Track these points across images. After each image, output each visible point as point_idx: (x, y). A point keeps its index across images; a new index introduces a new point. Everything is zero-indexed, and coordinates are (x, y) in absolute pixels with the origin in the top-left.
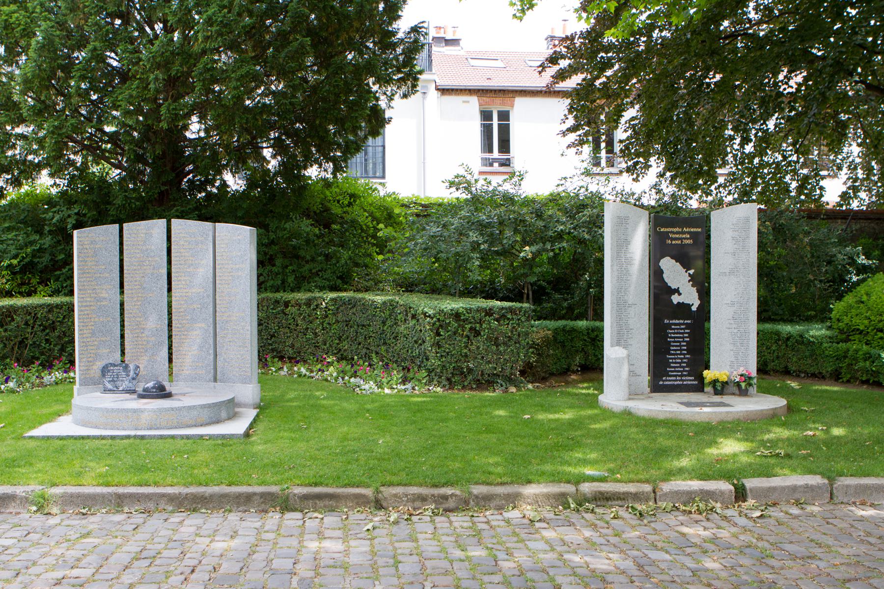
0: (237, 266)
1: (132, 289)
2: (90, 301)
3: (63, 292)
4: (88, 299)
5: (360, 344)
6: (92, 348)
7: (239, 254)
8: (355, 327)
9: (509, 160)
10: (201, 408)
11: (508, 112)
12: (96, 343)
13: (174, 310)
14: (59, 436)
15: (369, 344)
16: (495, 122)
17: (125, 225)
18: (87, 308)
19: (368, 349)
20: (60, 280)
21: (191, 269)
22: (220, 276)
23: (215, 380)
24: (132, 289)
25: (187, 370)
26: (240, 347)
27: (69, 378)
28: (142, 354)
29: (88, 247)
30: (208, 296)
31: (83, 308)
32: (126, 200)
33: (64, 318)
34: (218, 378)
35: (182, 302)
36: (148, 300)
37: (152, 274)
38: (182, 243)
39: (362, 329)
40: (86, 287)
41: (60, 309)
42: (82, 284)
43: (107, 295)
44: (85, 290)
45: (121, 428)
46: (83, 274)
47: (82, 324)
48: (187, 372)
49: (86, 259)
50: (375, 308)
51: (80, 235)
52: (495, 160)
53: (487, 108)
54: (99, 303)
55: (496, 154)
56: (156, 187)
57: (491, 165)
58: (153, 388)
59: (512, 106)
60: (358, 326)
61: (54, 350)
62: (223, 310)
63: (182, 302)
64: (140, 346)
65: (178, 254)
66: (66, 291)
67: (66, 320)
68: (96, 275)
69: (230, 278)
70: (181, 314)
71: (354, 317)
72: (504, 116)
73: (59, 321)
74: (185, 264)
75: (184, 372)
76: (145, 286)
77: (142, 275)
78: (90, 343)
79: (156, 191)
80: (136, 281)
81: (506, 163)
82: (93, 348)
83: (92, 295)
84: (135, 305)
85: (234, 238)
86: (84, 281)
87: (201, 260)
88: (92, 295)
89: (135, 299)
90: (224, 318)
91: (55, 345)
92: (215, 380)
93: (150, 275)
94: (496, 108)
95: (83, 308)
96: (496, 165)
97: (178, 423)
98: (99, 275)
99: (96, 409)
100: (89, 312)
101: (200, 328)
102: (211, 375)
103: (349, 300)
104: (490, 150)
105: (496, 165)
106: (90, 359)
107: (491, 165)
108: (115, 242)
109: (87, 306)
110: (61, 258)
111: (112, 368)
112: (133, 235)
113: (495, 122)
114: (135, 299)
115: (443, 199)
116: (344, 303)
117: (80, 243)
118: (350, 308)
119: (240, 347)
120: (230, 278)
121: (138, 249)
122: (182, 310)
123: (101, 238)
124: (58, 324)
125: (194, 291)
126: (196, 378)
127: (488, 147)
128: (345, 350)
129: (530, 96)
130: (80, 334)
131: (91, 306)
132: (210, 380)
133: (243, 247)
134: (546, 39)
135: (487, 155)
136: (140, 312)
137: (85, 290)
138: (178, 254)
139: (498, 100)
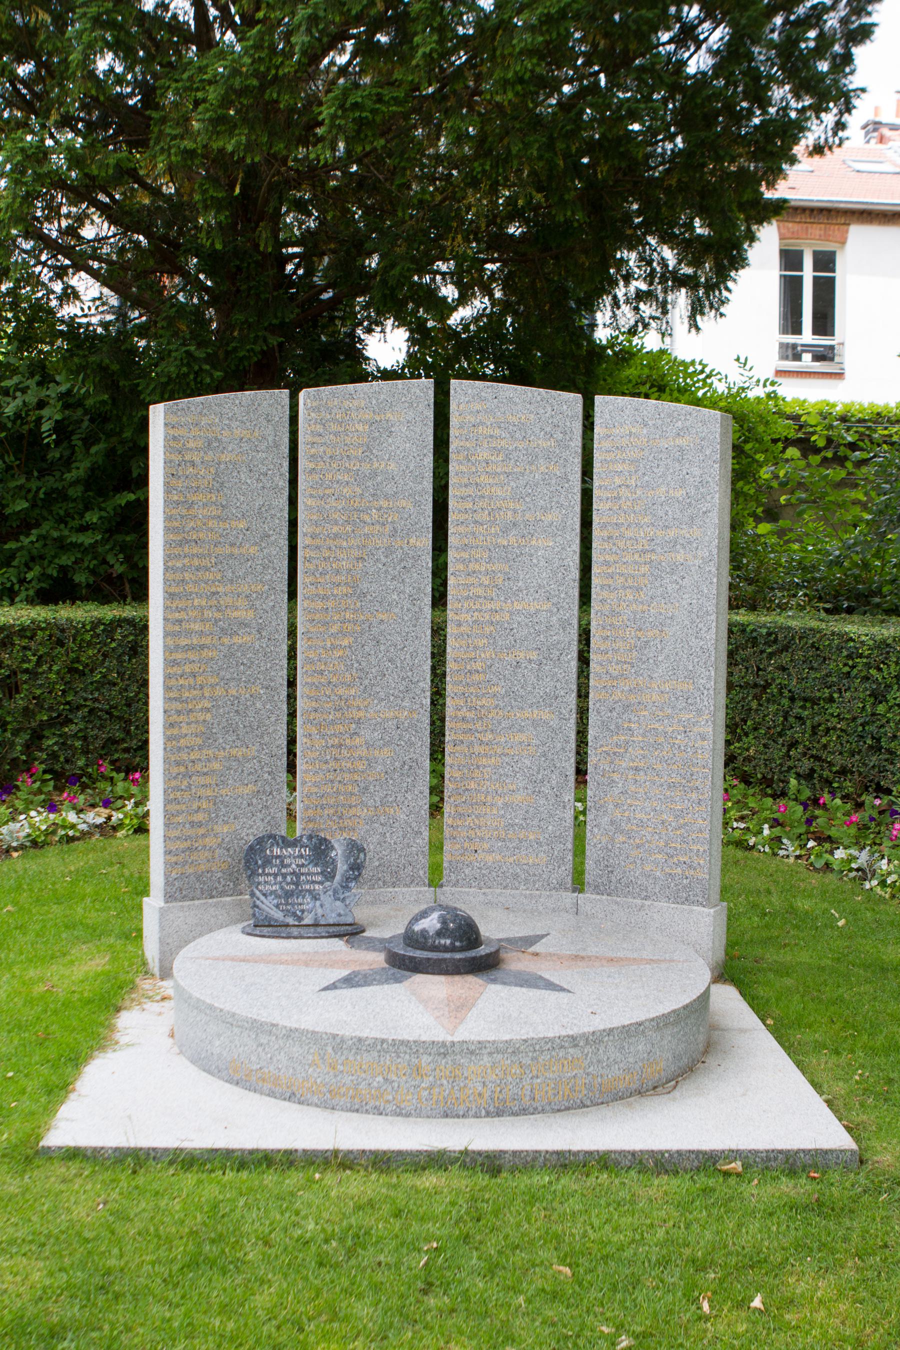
0: (672, 533)
1: (325, 598)
2: (201, 633)
3: (23, 595)
4: (197, 627)
5: (793, 744)
6: (203, 780)
7: (679, 494)
8: (785, 702)
9: (832, 348)
10: (658, 1028)
11: (833, 254)
12: (216, 766)
13: (451, 666)
14: (178, 1151)
15: (825, 747)
16: (808, 274)
17: (302, 395)
18: (191, 655)
19: (817, 758)
20: (15, 563)
21: (512, 539)
22: (607, 563)
23: (578, 884)
24: (325, 598)
25: (490, 851)
26: (671, 786)
27: (64, 827)
28: (353, 801)
29: (197, 460)
30: (564, 625)
31: (179, 656)
32: (188, 365)
33: (39, 663)
34: (588, 878)
35: (481, 642)
36: (374, 631)
37: (389, 551)
38: (484, 454)
39: (803, 707)
40: (190, 588)
41: (31, 638)
42: (179, 576)
43: (251, 614)
44: (188, 596)
45: (390, 1107)
46: (180, 544)
47: (178, 705)
48: (490, 858)
49: (192, 498)
50: (849, 657)
51: (174, 419)
52: (807, 348)
53: (793, 245)
54: (226, 640)
55: (807, 336)
56: (257, 337)
57: (797, 357)
58: (439, 934)
59: (843, 242)
60: (792, 699)
61: (12, 744)
62: (614, 670)
63: (481, 642)
64: (347, 776)
65: (470, 491)
66: (31, 592)
67: (45, 667)
68: (219, 550)
69: (644, 569)
70: (476, 677)
71: (780, 678)
72: (825, 261)
73: (26, 671)
74: (493, 523)
75: (481, 855)
76: (364, 586)
77: (356, 553)
78: (198, 767)
79: (257, 348)
80: (338, 572)
81: (824, 355)
82: (208, 780)
83: (208, 614)
84: (333, 647)
85: (664, 444)
86: (184, 569)
87: (545, 510)
88: (208, 614)
89: (334, 629)
90: (618, 695)
91: (16, 733)
92: (578, 884)
93: (380, 554)
94: (809, 245)
95: (179, 656)
96: (807, 357)
97: (590, 1087)
98: (228, 550)
99: (291, 1034)
100: (195, 667)
101: (535, 724)
102: (565, 871)
103: (769, 634)
104: (797, 329)
105: (807, 357)
106: (200, 817)
107: (797, 357)
108: (277, 446)
109: (190, 648)
110: (18, 508)
111: (277, 851)
112: (334, 427)
113: (808, 274)
114: (334, 629)
115: (834, 406)
116: (754, 642)
117: (171, 442)
118: (771, 656)
119: (671, 786)
120: (644, 569)
121: (348, 471)
122: (478, 666)
123: (237, 432)
124: (25, 677)
125: (518, 606)
126: (516, 876)
127: (791, 323)
128: (748, 759)
129: (880, 223)
130: (168, 739)
131: (202, 647)
132: (561, 885)
133: (696, 471)
134: (864, 127)
135: (791, 339)
136: (348, 668)
137: (188, 596)
138: (470, 491)
139: (816, 230)
